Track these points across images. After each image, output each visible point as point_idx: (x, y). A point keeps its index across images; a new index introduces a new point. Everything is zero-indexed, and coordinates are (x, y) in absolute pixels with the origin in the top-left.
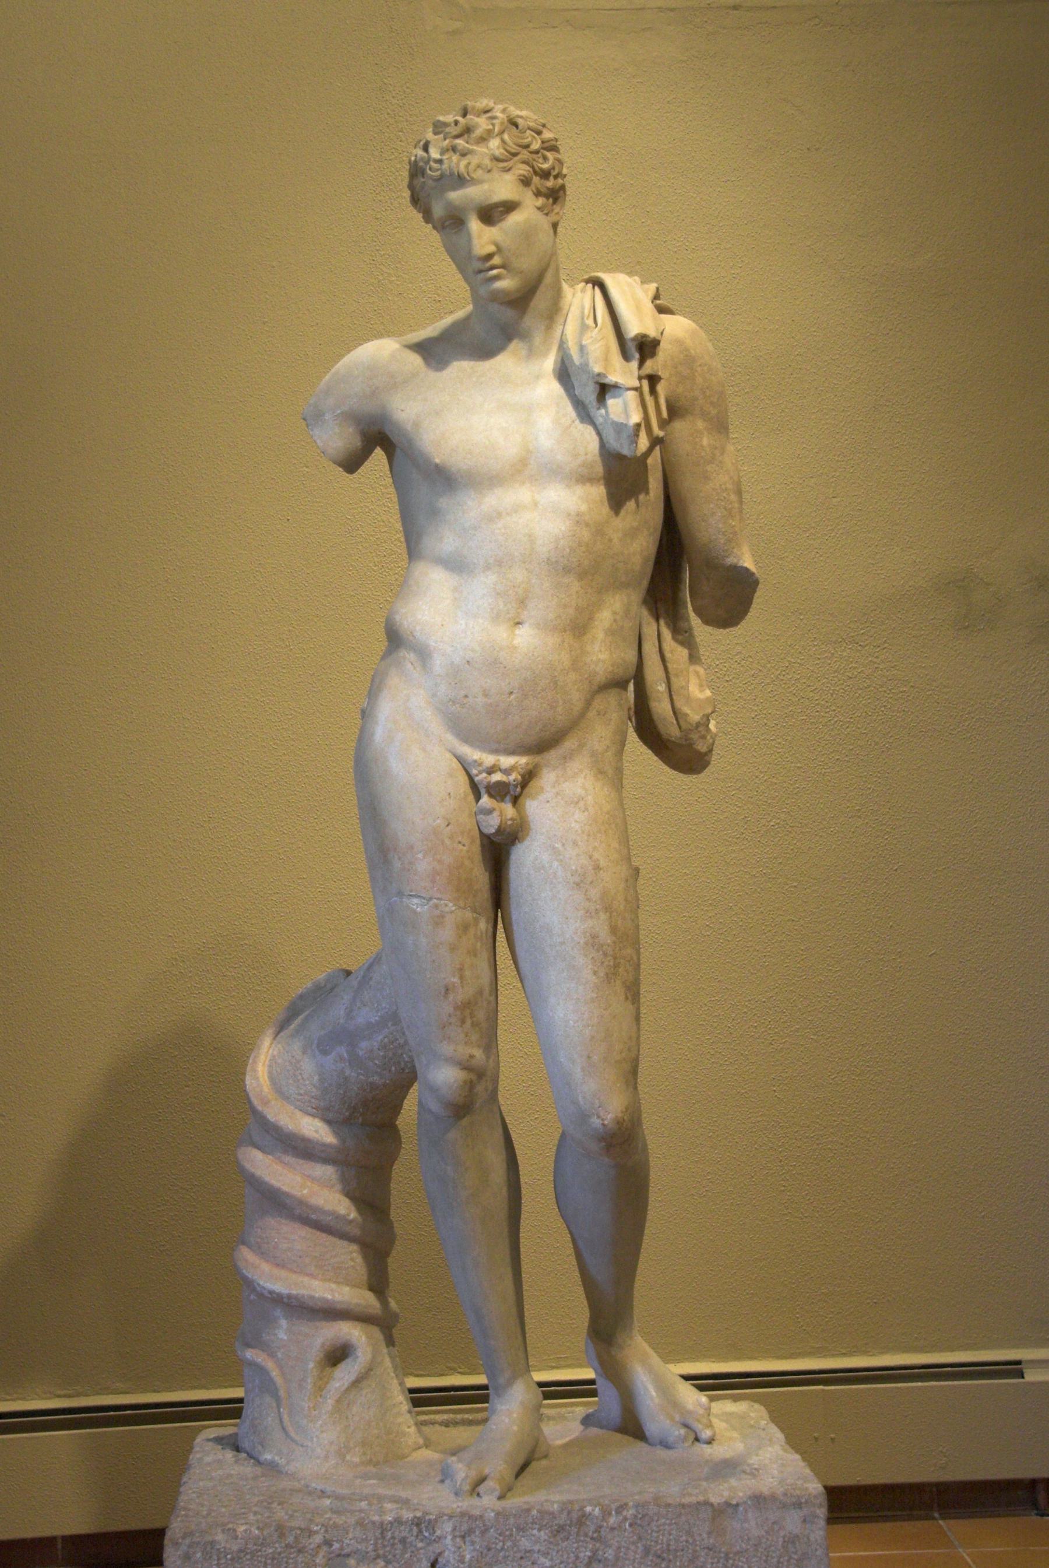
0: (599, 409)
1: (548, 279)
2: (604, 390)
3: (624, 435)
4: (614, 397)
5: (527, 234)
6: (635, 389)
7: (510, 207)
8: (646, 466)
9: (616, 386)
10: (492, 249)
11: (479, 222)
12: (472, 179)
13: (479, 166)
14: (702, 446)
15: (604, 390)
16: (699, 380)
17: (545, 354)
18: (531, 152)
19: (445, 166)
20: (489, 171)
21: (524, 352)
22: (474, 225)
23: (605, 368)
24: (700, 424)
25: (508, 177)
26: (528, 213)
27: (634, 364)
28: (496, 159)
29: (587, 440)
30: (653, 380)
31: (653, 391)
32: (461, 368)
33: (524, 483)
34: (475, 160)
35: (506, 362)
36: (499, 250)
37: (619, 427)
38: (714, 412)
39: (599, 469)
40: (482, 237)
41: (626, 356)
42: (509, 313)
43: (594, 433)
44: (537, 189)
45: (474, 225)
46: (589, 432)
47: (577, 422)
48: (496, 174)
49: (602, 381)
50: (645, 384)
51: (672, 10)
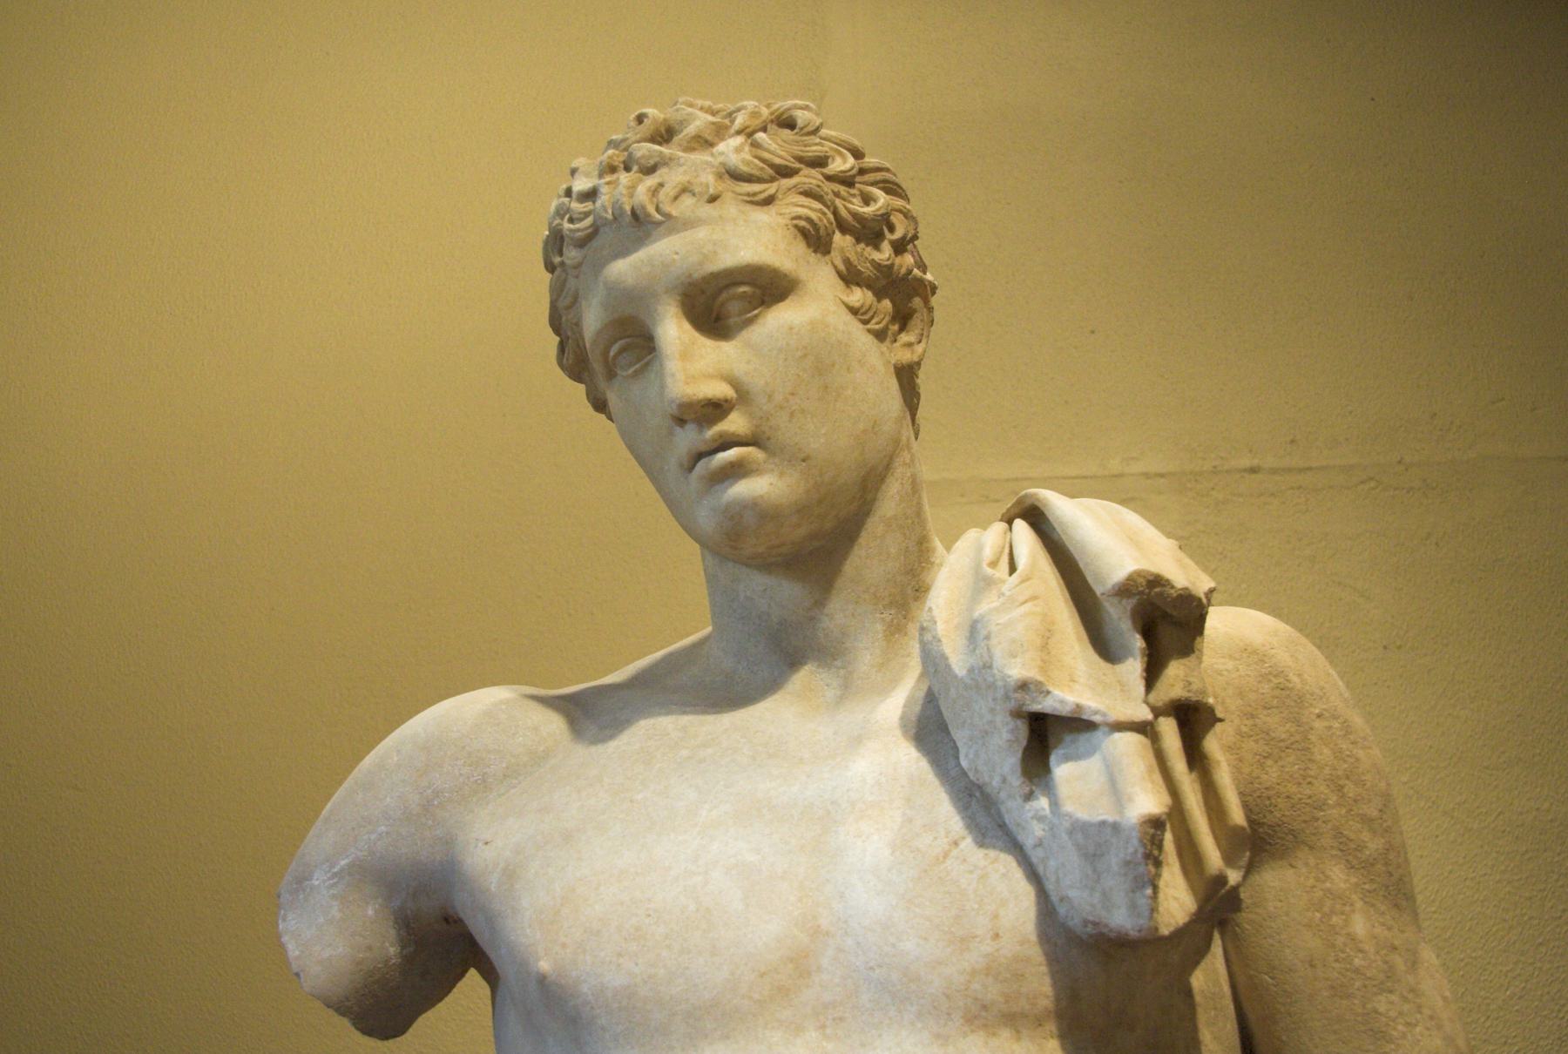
0: (1029, 797)
1: (889, 503)
2: (1045, 734)
3: (1114, 861)
4: (1067, 758)
5: (818, 362)
6: (1143, 728)
7: (769, 288)
8: (1188, 993)
9: (1079, 724)
10: (721, 390)
11: (687, 326)
12: (668, 216)
13: (685, 190)
14: (1352, 938)
15: (1045, 734)
16: (1323, 754)
17: (884, 690)
18: (829, 178)
19: (604, 199)
20: (713, 199)
21: (830, 694)
22: (673, 330)
23: (1044, 669)
24: (1339, 877)
25: (762, 216)
26: (820, 307)
27: (1133, 668)
28: (736, 176)
29: (1002, 900)
30: (1192, 718)
31: (1195, 756)
32: (658, 732)
33: (799, 1029)
34: (672, 178)
35: (779, 716)
36: (743, 396)
37: (1093, 839)
38: (1374, 845)
39: (1040, 986)
40: (691, 362)
41: (1105, 647)
42: (784, 594)
43: (1018, 874)
44: (847, 261)
45: (673, 330)
46: (1004, 874)
47: (968, 843)
48: (731, 207)
49: (1037, 708)
50: (1169, 729)
51: (1162, 476)
